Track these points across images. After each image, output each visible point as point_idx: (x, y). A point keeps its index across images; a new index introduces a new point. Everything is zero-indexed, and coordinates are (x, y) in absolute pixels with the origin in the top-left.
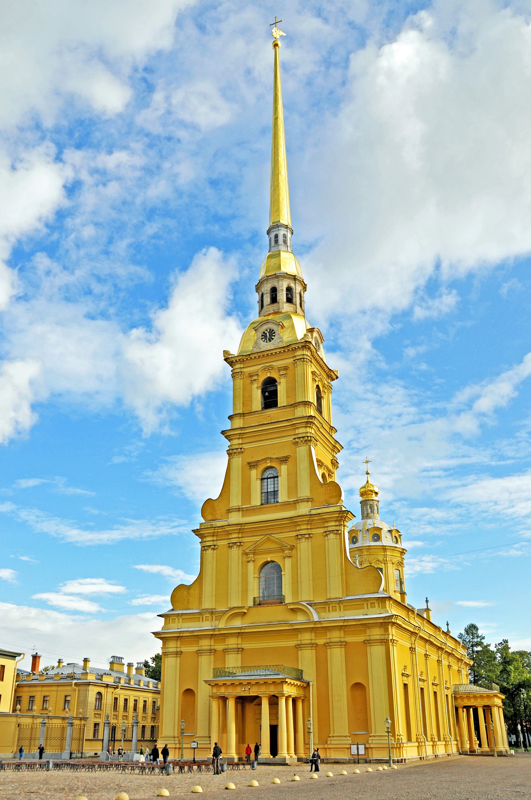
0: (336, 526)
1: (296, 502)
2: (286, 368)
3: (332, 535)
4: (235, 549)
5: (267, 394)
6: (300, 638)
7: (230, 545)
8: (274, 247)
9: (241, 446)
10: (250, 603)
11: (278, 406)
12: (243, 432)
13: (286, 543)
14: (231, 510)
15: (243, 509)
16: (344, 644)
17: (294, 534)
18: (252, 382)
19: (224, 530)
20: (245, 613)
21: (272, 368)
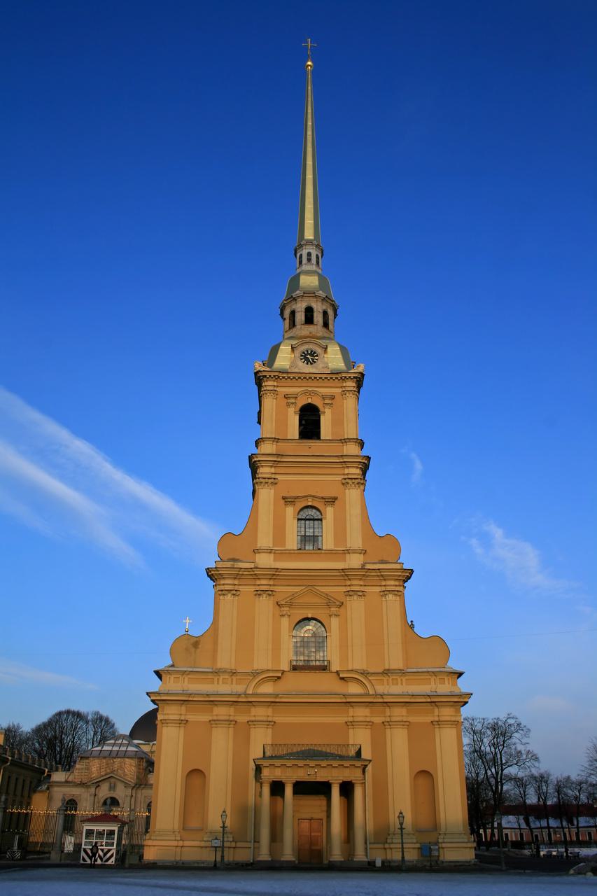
0: (396, 586)
1: (348, 551)
2: (332, 398)
3: (390, 596)
4: (264, 598)
5: (303, 422)
6: (351, 714)
7: (259, 593)
8: (305, 264)
9: (273, 476)
10: (285, 667)
11: (322, 437)
12: (279, 460)
13: (335, 599)
14: (260, 551)
15: (277, 552)
16: (407, 725)
17: (344, 589)
18: (288, 404)
19: (252, 573)
20: (279, 678)
21: (315, 393)
